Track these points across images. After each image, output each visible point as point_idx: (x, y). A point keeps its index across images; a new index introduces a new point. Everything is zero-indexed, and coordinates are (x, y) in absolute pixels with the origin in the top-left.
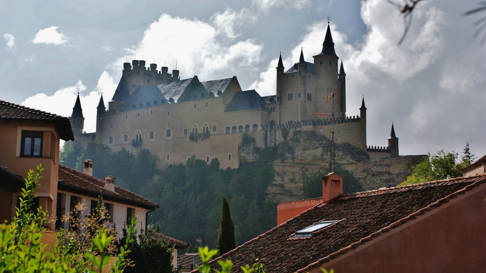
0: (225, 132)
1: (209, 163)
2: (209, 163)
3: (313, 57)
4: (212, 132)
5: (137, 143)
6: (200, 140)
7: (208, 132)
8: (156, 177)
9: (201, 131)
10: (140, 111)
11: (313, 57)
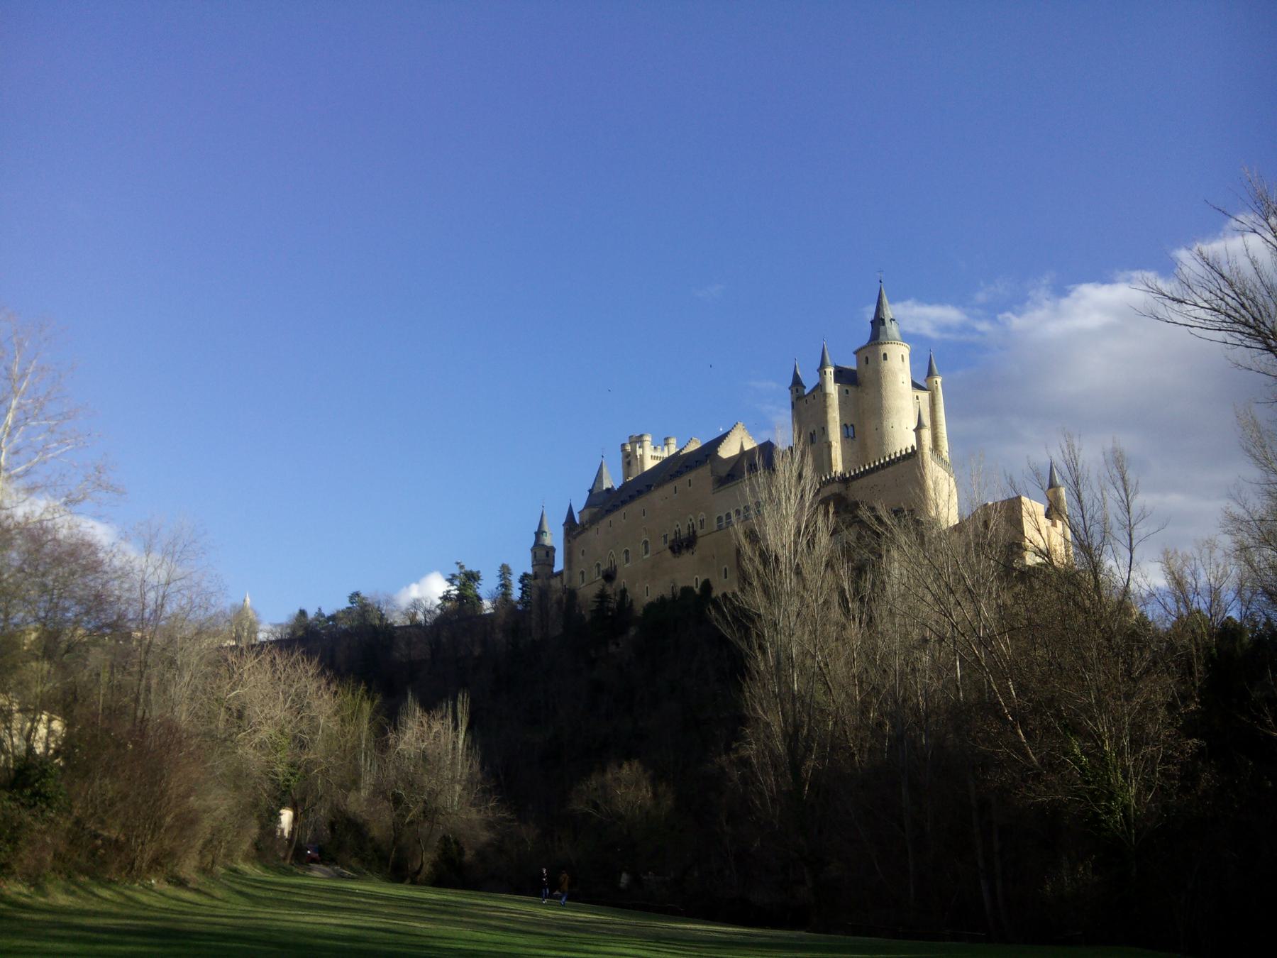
0: (716, 528)
1: (697, 590)
2: (697, 590)
3: (855, 353)
4: (699, 532)
5: (609, 576)
6: (684, 551)
7: (694, 532)
8: (632, 632)
9: (684, 532)
10: (611, 518)
11: (855, 353)
